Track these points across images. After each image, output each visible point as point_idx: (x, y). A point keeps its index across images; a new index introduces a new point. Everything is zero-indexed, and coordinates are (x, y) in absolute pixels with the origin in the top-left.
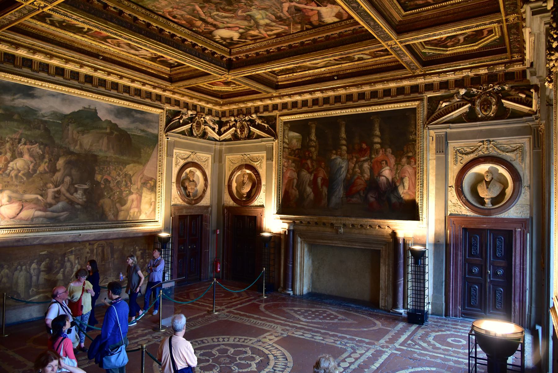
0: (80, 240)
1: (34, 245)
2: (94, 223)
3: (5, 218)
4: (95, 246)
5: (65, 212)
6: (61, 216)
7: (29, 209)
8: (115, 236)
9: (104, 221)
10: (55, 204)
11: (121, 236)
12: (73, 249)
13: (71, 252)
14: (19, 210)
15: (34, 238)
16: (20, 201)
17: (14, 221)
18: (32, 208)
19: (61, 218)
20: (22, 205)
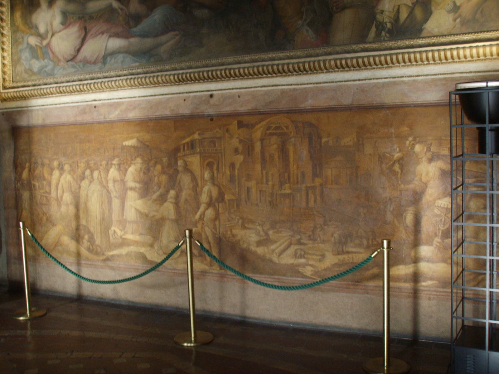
0: (211, 111)
1: (112, 122)
2: (247, 58)
3: (59, 60)
4: (258, 133)
5: (172, 34)
6: (161, 45)
7: (96, 35)
8: (322, 102)
9: (281, 48)
10: (147, 16)
11: (346, 101)
12: (196, 136)
13: (192, 145)
14: (80, 40)
15: (111, 105)
16: (80, 18)
17: (74, 67)
18: (103, 33)
19: (162, 49)
20: (85, 28)
